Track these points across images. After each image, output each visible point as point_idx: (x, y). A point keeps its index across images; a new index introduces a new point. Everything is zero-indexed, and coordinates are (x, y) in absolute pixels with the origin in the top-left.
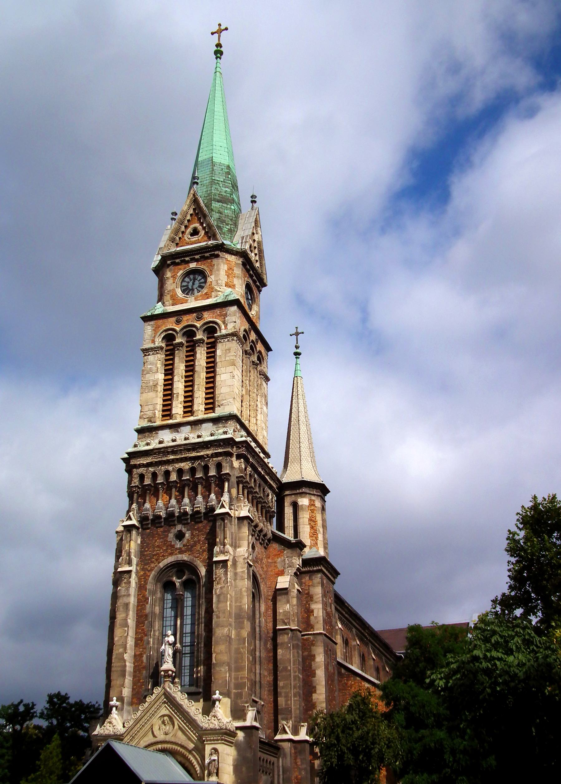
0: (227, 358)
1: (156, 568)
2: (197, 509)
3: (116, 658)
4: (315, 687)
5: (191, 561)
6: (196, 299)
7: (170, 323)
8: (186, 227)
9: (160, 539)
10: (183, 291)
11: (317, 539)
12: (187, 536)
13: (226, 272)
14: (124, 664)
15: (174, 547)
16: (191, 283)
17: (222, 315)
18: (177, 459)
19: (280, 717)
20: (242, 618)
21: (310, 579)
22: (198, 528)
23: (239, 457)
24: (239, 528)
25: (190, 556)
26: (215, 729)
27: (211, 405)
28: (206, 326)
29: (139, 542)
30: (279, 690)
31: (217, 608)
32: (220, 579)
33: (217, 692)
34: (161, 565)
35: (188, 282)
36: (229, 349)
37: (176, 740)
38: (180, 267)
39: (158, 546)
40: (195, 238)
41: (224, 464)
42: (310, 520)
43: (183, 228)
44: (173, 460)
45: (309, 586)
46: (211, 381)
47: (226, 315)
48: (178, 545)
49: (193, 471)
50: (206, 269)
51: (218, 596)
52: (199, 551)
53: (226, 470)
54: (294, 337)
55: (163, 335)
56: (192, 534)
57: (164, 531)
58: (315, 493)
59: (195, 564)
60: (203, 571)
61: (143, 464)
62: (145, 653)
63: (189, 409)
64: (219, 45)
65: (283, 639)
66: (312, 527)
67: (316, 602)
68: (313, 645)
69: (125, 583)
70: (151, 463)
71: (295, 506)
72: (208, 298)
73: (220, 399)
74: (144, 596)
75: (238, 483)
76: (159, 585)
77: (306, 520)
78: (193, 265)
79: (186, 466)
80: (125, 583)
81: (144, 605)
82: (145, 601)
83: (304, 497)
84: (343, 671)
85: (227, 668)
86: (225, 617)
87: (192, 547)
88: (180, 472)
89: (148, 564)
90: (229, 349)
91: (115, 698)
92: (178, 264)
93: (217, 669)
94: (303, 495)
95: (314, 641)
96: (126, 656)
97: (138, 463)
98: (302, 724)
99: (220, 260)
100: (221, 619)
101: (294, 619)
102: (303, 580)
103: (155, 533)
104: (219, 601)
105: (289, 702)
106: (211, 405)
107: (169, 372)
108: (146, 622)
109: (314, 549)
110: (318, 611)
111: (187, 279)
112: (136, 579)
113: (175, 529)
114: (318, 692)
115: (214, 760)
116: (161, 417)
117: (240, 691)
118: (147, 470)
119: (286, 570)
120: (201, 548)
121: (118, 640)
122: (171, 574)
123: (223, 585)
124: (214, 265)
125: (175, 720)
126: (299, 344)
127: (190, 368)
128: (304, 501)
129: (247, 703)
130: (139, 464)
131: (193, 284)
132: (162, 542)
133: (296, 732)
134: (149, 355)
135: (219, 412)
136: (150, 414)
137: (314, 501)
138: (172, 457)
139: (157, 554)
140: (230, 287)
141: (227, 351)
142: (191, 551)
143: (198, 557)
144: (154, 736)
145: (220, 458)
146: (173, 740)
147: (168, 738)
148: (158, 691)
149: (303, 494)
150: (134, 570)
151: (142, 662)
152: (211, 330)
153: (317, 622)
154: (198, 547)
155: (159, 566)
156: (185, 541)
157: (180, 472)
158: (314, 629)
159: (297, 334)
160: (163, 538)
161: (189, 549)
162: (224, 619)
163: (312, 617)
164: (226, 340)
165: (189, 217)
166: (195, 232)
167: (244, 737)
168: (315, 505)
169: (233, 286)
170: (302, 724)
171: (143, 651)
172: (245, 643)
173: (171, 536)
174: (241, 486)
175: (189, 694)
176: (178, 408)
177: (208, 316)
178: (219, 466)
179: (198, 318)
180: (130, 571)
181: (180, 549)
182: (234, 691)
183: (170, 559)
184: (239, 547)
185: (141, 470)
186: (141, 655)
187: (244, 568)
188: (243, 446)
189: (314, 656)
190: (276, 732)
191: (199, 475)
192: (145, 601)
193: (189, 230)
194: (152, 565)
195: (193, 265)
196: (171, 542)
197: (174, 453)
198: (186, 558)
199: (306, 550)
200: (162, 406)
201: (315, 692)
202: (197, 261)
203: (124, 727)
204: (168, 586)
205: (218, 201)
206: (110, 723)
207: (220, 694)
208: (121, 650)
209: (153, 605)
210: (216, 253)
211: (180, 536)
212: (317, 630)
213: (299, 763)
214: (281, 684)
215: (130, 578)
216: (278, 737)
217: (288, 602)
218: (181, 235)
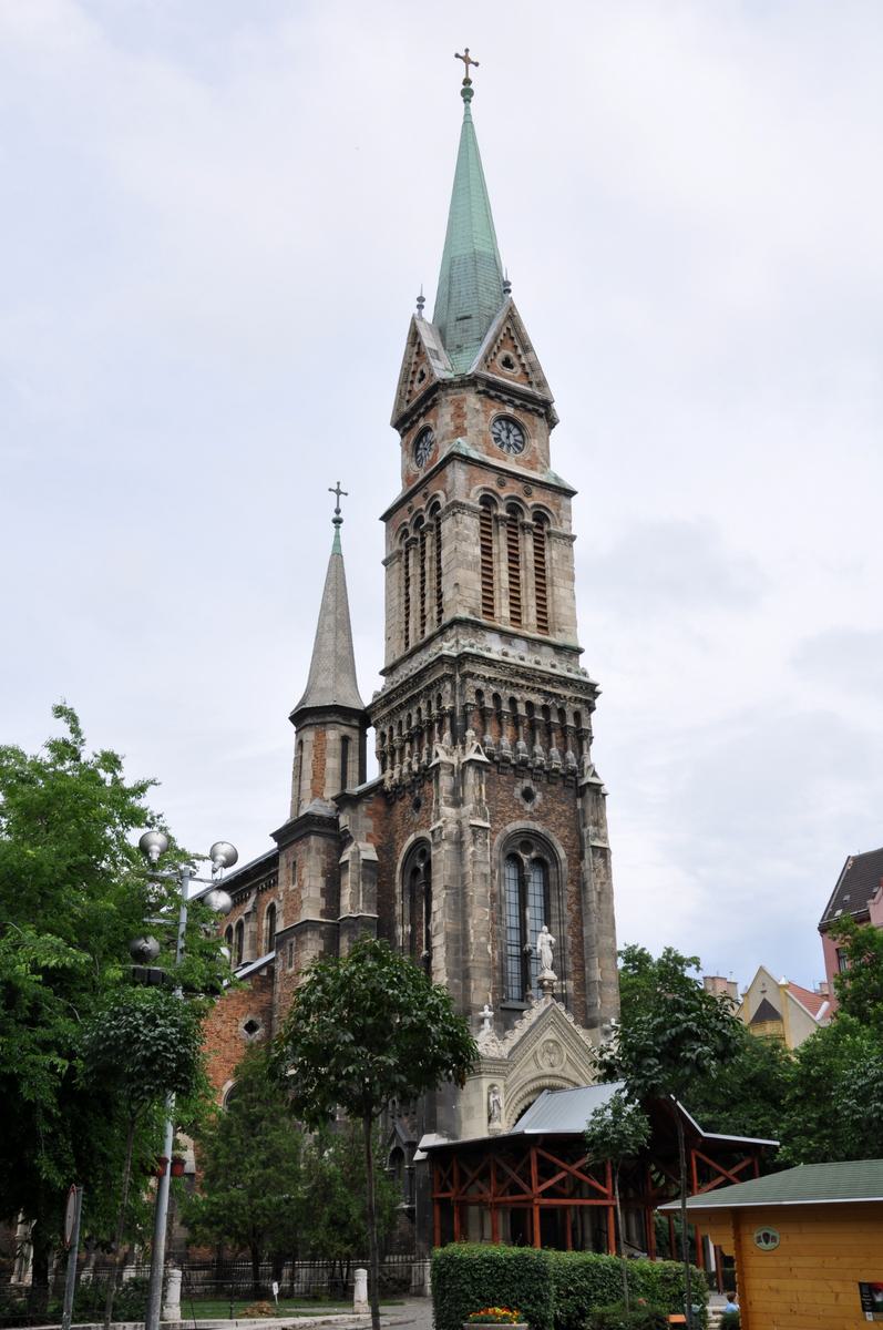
7: (490, 481)
12: (539, 797)
27: (543, 624)
32: (600, 871)
37: (563, 1075)
38: (493, 403)
39: (502, 801)
40: (508, 371)
43: (495, 349)
44: (523, 686)
46: (541, 588)
48: (528, 807)
49: (545, 710)
51: (599, 893)
56: (544, 798)
60: (562, 854)
63: (516, 618)
64: (467, 82)
70: (495, 679)
72: (532, 469)
78: (510, 410)
79: (538, 700)
87: (545, 816)
88: (529, 705)
91: (486, 1007)
92: (491, 398)
106: (543, 624)
111: (497, 424)
125: (564, 1048)
127: (514, 558)
130: (478, 676)
138: (523, 682)
144: (539, 1067)
145: (579, 706)
147: (556, 1070)
152: (541, 517)
161: (541, 816)
164: (562, 541)
165: (502, 337)
166: (507, 363)
173: (518, 792)
176: (503, 610)
181: (531, 813)
183: (519, 824)
185: (480, 684)
195: (510, 410)
197: (523, 676)
198: (539, 829)
202: (516, 407)
204: (513, 858)
211: (528, 795)
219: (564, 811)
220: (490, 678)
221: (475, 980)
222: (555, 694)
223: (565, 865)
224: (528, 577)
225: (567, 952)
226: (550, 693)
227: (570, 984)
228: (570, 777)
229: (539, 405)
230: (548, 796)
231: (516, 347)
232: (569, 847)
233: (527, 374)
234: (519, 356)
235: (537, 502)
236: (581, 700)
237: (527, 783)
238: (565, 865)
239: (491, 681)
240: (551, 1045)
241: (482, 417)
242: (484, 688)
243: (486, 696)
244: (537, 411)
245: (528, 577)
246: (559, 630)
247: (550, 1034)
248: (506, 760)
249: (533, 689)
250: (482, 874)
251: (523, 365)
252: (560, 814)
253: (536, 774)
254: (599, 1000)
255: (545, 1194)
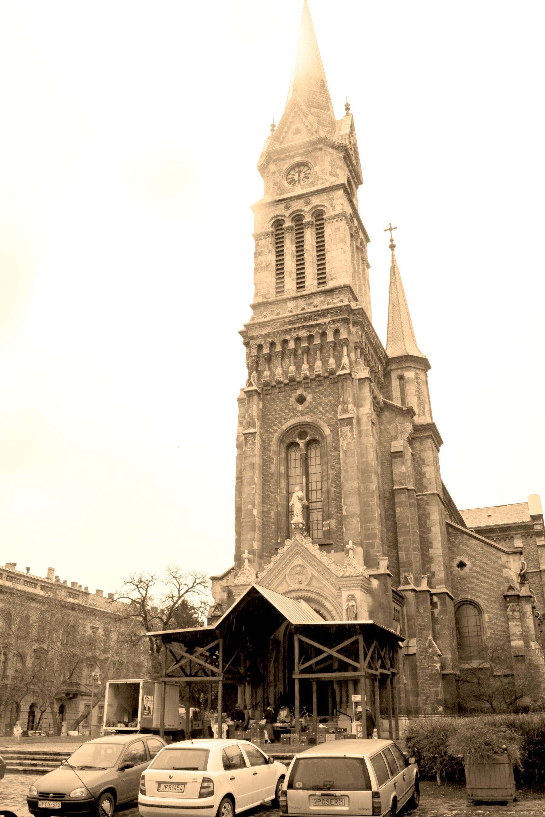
0: (337, 236)
1: (279, 430)
2: (317, 373)
3: (245, 514)
4: (431, 543)
5: (314, 422)
6: (302, 188)
8: (289, 128)
9: (282, 403)
10: (290, 183)
11: (424, 408)
12: (309, 398)
13: (330, 163)
14: (253, 519)
15: (296, 410)
16: (297, 175)
17: (330, 199)
18: (295, 328)
19: (401, 569)
20: (369, 473)
21: (421, 444)
22: (320, 391)
23: (355, 323)
24: (360, 389)
25: (313, 417)
26: (352, 576)
28: (314, 210)
29: (261, 407)
30: (399, 545)
31: (345, 463)
32: (346, 436)
33: (350, 542)
34: (284, 427)
35: (294, 175)
36: (339, 228)
38: (285, 162)
39: (280, 410)
41: (342, 330)
42: (417, 391)
43: (286, 129)
44: (290, 330)
45: (420, 451)
46: (321, 258)
47: (333, 199)
48: (300, 407)
49: (311, 338)
50: (310, 161)
51: (345, 452)
52: (321, 412)
53: (344, 335)
54: (389, 232)
55: (272, 221)
56: (314, 397)
57: (286, 396)
58: (419, 367)
59: (318, 424)
60: (327, 431)
61: (261, 335)
62: (273, 509)
65: (401, 498)
66: (419, 398)
67: (428, 465)
68: (427, 504)
69: (250, 444)
70: (269, 333)
71: (401, 378)
72: (314, 186)
73: (332, 273)
74: (269, 457)
75: (356, 349)
76: (284, 446)
77: (413, 392)
79: (303, 333)
80: (250, 444)
81: (269, 465)
82: (270, 461)
83: (410, 370)
84: (451, 530)
85: (359, 519)
86: (353, 471)
87: (314, 409)
88: (298, 340)
89: (271, 426)
90: (339, 228)
91: (246, 551)
93: (347, 520)
94: (409, 369)
95: (427, 500)
96: (255, 512)
97: (256, 334)
98: (423, 576)
99: (323, 153)
100: (349, 473)
101: (410, 480)
102: (414, 446)
103: (276, 398)
104: (346, 456)
105: (410, 556)
107: (280, 253)
108: (272, 480)
109: (423, 417)
110: (431, 473)
112: (260, 441)
113: (296, 393)
114: (434, 547)
115: (353, 606)
116: (274, 293)
117: (371, 541)
118: (265, 341)
119: (399, 436)
120: (323, 409)
121: (246, 498)
122: (293, 436)
123: (349, 441)
124: (318, 157)
126: (393, 238)
128: (409, 375)
129: (379, 552)
130: (257, 336)
131: (299, 176)
132: (283, 406)
133: (418, 582)
134: (260, 239)
135: (330, 285)
136: (264, 291)
137: (419, 374)
139: (280, 417)
140: (334, 176)
141: (337, 230)
142: (313, 413)
143: (320, 418)
144: (289, 586)
146: (308, 588)
147: (302, 586)
148: (288, 543)
149: (408, 368)
150: (258, 432)
151: (271, 518)
153: (430, 484)
154: (320, 408)
155: (283, 429)
156: (306, 404)
157: (298, 340)
158: (427, 490)
159: (391, 229)
160: (284, 402)
161: (311, 411)
162: (353, 473)
163: (425, 480)
164: (335, 220)
165: (290, 119)
167: (378, 585)
168: (419, 378)
169: (337, 176)
170: (423, 576)
171: (270, 508)
172: (373, 496)
173: (292, 400)
174: (359, 351)
175: (320, 545)
176: (290, 284)
177: (315, 201)
178: (337, 332)
179: (306, 203)
180: (255, 433)
181: (302, 411)
182: (366, 541)
183: (293, 421)
184: (361, 407)
186: (269, 511)
187: (369, 425)
188: (359, 313)
189: (429, 514)
190: (399, 583)
191: (317, 341)
192: (270, 461)
193: (291, 131)
194: (275, 428)
196: (293, 405)
199: (416, 418)
200: (275, 284)
201: (432, 547)
203: (257, 577)
205: (316, 108)
206: (244, 573)
207: (353, 543)
208: (250, 506)
209: (278, 465)
210: (320, 146)
211: (301, 400)
212: (430, 491)
213: (422, 611)
214: (400, 539)
215: (255, 439)
216: (401, 588)
217: (403, 464)
218: (284, 135)
219: (330, 401)
220: (265, 334)
221: (243, 535)
222: (317, 325)
223: (329, 439)
224: (310, 256)
225: (330, 500)
226: (312, 326)
227: (333, 522)
228: (332, 377)
229: (317, 144)
230: (316, 395)
231: (302, 119)
232: (333, 425)
233: (310, 130)
234: (304, 123)
235: (313, 205)
236: (338, 321)
237: (300, 392)
238: (329, 439)
239: (267, 335)
240: (298, 568)
241: (277, 174)
242: (263, 343)
243: (265, 346)
244: (316, 149)
245: (310, 256)
246: (332, 279)
247: (298, 561)
248: (279, 382)
249: (299, 328)
250: (251, 463)
251: (307, 126)
252: (326, 405)
253: (305, 383)
254: (344, 529)
255: (303, 671)
